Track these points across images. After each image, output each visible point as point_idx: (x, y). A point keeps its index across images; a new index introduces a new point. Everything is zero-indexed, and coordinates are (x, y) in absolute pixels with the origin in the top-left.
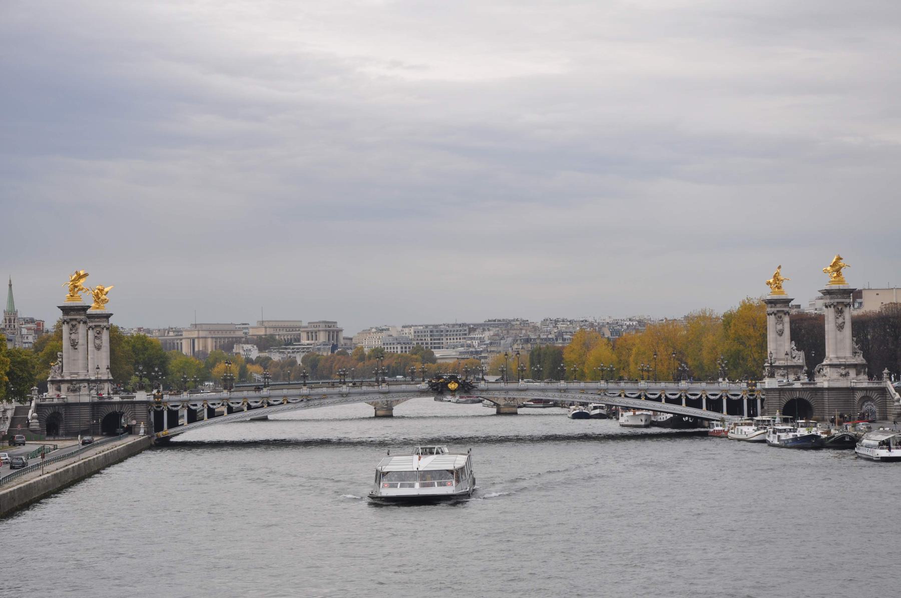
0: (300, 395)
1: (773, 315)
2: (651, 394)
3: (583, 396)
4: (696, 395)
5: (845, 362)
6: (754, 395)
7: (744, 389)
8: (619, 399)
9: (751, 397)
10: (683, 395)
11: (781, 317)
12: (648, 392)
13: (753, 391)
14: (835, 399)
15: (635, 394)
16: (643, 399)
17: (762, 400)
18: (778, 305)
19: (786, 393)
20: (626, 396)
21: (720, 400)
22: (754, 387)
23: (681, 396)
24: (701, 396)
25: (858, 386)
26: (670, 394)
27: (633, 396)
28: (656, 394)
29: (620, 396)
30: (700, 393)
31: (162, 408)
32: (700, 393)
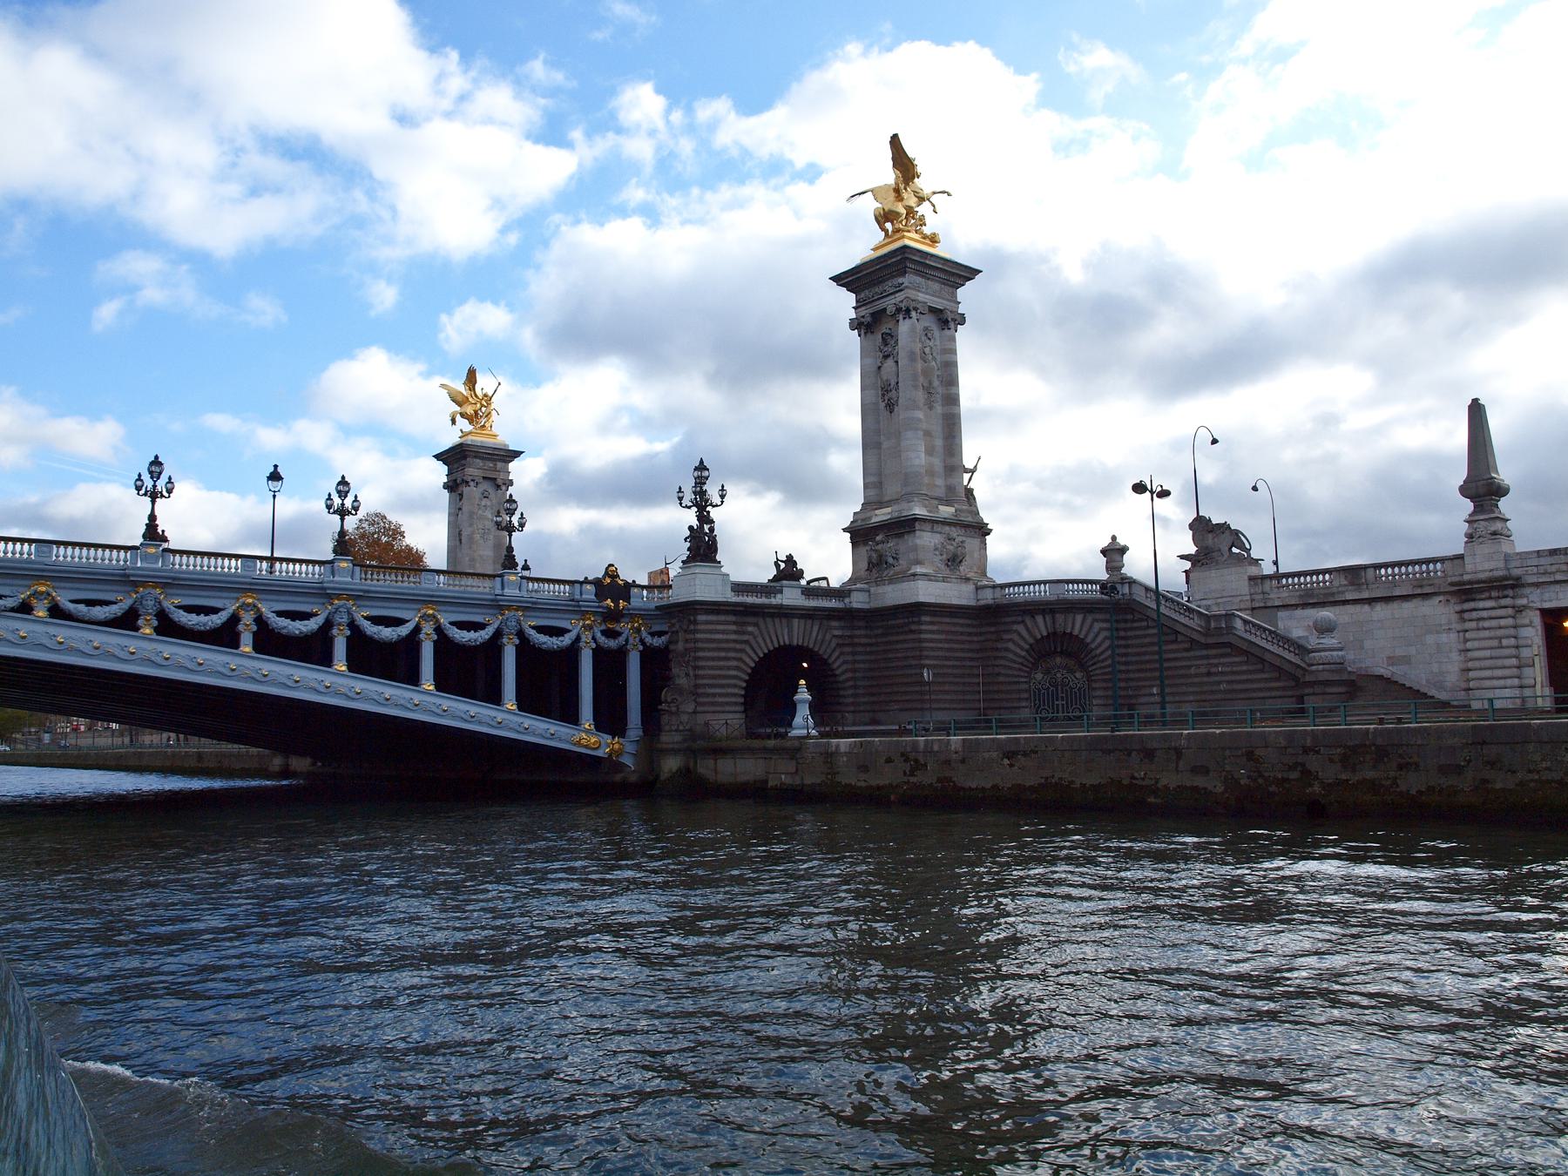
2: (189, 609)
4: (399, 622)
6: (619, 634)
9: (612, 644)
10: (337, 619)
17: (649, 655)
20: (56, 612)
21: (493, 648)
23: (328, 624)
24: (417, 629)
26: (280, 614)
27: (99, 612)
28: (215, 611)
29: (25, 608)
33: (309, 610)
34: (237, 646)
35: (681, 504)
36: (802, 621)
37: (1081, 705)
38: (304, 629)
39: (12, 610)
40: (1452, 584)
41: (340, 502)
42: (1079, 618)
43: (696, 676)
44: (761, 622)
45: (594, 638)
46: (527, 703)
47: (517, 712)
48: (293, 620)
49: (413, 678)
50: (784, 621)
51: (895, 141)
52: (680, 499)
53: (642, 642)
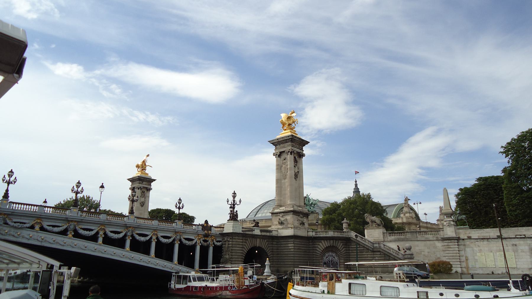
1: (140, 189)
4: (146, 236)
5: (302, 210)
6: (208, 241)
8: (29, 232)
9: (205, 244)
11: (143, 192)
12: (80, 226)
14: (298, 249)
15: (59, 226)
16: (70, 234)
17: (216, 248)
18: (144, 183)
19: (247, 240)
23: (125, 235)
24: (151, 238)
25: (321, 236)
26: (112, 232)
27: (56, 229)
28: (92, 230)
29: (32, 227)
33: (120, 231)
35: (228, 203)
37: (337, 267)
38: (119, 237)
39: (28, 228)
40: (442, 238)
41: (133, 198)
43: (232, 255)
45: (200, 242)
47: (178, 264)
48: (115, 234)
52: (228, 202)
53: (214, 243)
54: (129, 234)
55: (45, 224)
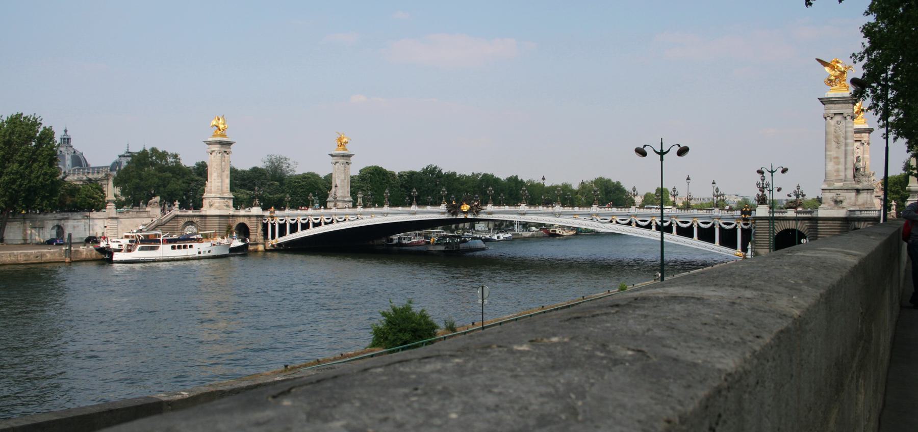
0: (356, 214)
2: (641, 221)
3: (576, 221)
4: (687, 222)
6: (748, 224)
7: (738, 217)
9: (746, 227)
13: (747, 220)
16: (634, 225)
21: (712, 229)
22: (747, 216)
23: (671, 223)
27: (624, 222)
28: (646, 221)
29: (611, 222)
30: (691, 221)
31: (274, 221)
32: (691, 221)
34: (651, 229)
36: (794, 222)
42: (863, 223)
44: (779, 222)
46: (723, 243)
49: (691, 236)
50: (788, 221)
51: (818, 60)
54: (674, 222)
55: (618, 219)
